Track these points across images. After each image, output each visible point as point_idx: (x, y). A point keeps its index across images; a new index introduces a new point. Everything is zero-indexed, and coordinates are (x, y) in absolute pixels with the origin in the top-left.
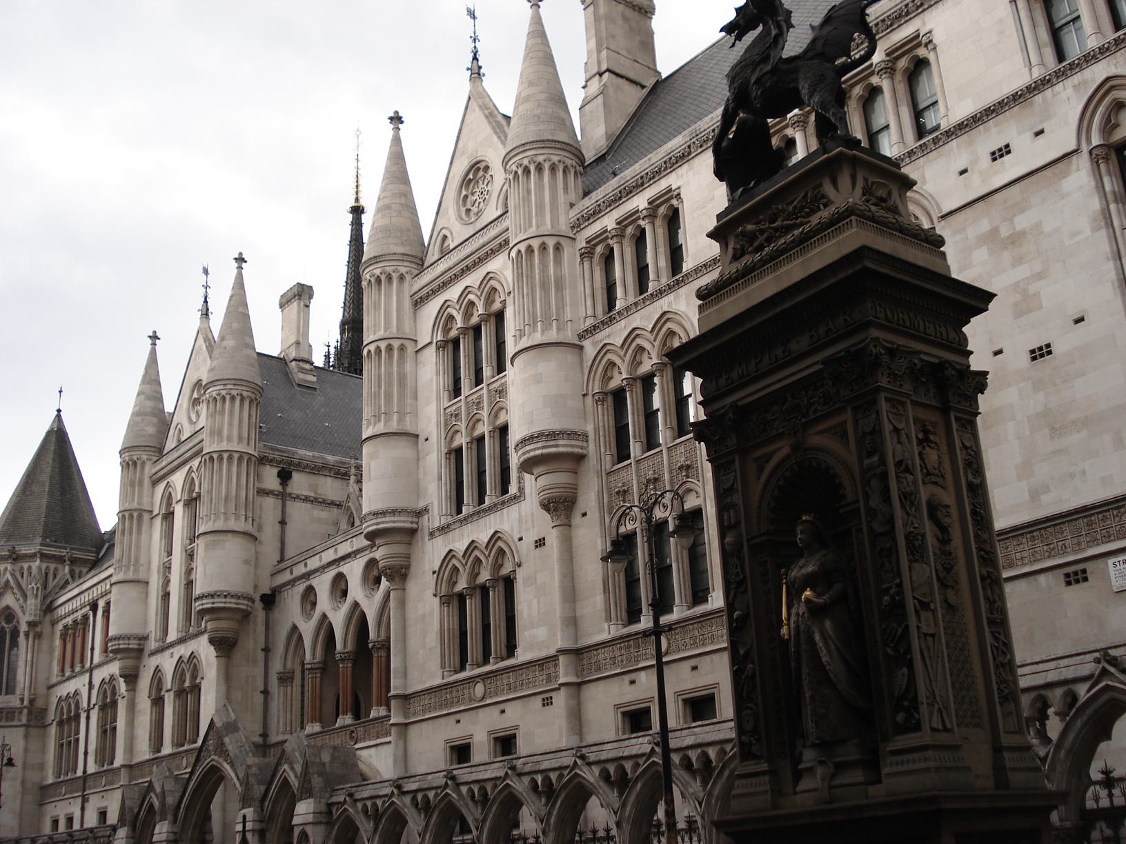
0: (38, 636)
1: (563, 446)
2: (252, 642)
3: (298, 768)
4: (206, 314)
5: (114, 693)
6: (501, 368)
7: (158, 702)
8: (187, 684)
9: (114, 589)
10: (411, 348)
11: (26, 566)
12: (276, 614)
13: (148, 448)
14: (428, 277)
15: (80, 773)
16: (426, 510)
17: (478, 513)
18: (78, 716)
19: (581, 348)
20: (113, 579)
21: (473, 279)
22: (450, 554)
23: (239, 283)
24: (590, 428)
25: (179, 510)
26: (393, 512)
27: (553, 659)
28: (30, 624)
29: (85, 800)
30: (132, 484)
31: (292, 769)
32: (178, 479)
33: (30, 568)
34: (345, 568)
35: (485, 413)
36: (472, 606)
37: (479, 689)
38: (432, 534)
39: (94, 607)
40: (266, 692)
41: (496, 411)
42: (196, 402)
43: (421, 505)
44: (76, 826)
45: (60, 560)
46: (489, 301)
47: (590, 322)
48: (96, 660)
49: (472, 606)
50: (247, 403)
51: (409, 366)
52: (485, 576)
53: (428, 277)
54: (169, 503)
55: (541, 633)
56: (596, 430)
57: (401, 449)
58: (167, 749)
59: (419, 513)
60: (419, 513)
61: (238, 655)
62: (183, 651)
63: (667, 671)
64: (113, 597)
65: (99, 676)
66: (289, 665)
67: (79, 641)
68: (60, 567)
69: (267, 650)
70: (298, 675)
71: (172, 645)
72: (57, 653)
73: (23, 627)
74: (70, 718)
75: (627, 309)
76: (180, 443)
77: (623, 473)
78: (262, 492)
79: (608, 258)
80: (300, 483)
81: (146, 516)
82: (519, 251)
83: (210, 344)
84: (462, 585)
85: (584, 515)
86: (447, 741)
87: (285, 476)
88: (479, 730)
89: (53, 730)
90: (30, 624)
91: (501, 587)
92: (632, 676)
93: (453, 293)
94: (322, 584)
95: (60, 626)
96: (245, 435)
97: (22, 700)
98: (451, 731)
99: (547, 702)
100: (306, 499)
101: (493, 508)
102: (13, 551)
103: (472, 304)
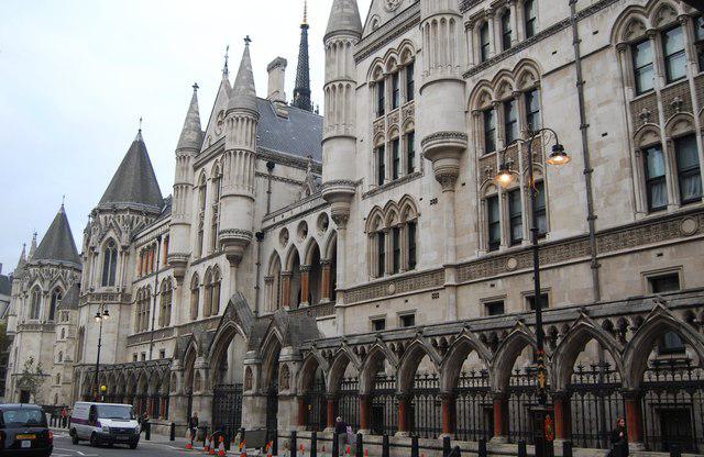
0: (128, 254)
1: (452, 142)
2: (251, 259)
3: (283, 330)
4: (226, 72)
5: (170, 287)
6: (410, 97)
7: (195, 291)
8: (213, 281)
9: (172, 229)
10: (353, 86)
13: (195, 149)
14: (365, 44)
15: (150, 330)
16: (360, 182)
17: (394, 183)
18: (149, 299)
19: (465, 83)
21: (395, 44)
22: (376, 208)
23: (246, 53)
24: (469, 132)
25: (209, 184)
26: (341, 182)
27: (441, 271)
28: (123, 247)
29: (152, 344)
30: (183, 169)
31: (279, 329)
32: (209, 167)
34: (305, 218)
35: (400, 124)
36: (388, 239)
37: (392, 288)
38: (364, 197)
39: (159, 238)
40: (257, 288)
41: (408, 121)
42: (220, 123)
43: (357, 179)
44: (147, 359)
45: (140, 213)
46: (404, 58)
47: (471, 67)
48: (160, 268)
49: (388, 239)
50: (250, 123)
51: (351, 98)
52: (397, 221)
53: (365, 44)
54: (204, 181)
55: (434, 255)
56: (474, 133)
57: (346, 145)
58: (200, 318)
59: (356, 185)
60: (356, 185)
61: (242, 266)
62: (211, 263)
63: (541, 274)
65: (161, 277)
67: (150, 258)
69: (258, 264)
70: (276, 278)
71: (205, 259)
72: (138, 263)
73: (119, 249)
74: (144, 299)
75: (497, 58)
76: (210, 146)
77: (490, 160)
78: (258, 174)
79: (484, 29)
80: (279, 170)
81: (190, 188)
83: (230, 92)
84: (382, 226)
85: (464, 184)
86: (370, 318)
87: (270, 166)
88: (391, 312)
89: (135, 306)
90: (123, 247)
91: (407, 228)
92: (493, 282)
93: (381, 53)
94: (293, 227)
95: (139, 250)
96: (249, 140)
99: (435, 296)
100: (282, 180)
101: (404, 180)
102: (114, 207)
103: (393, 59)
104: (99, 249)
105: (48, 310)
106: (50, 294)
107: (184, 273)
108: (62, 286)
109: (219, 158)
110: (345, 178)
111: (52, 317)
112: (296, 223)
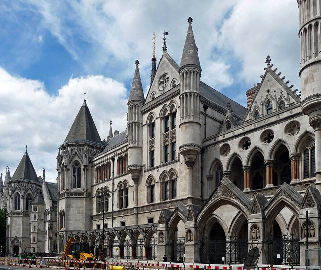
2: (198, 165)
7: (151, 188)
11: (81, 148)
12: (205, 156)
20: (130, 146)
28: (85, 166)
32: (157, 111)
33: (83, 149)
45: (93, 147)
64: (129, 152)
66: (211, 173)
68: (93, 150)
70: (214, 177)
74: (104, 195)
82: (305, 28)
89: (95, 199)
90: (85, 166)
95: (96, 167)
97: (84, 190)
98: (148, 215)
104: (70, 167)
105: (25, 205)
106: (25, 197)
107: (139, 177)
108: (31, 193)
109: (168, 103)
110: (312, 94)
111: (27, 209)
112: (258, 134)
